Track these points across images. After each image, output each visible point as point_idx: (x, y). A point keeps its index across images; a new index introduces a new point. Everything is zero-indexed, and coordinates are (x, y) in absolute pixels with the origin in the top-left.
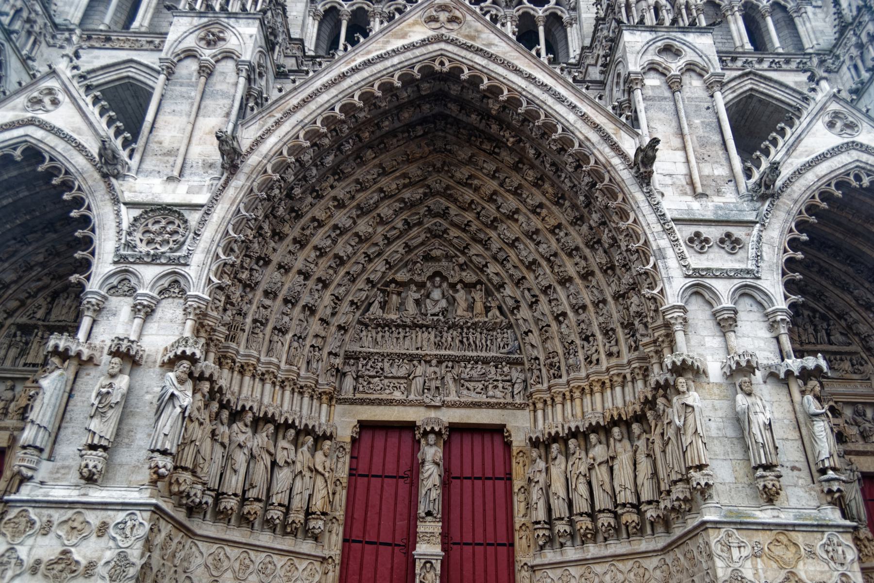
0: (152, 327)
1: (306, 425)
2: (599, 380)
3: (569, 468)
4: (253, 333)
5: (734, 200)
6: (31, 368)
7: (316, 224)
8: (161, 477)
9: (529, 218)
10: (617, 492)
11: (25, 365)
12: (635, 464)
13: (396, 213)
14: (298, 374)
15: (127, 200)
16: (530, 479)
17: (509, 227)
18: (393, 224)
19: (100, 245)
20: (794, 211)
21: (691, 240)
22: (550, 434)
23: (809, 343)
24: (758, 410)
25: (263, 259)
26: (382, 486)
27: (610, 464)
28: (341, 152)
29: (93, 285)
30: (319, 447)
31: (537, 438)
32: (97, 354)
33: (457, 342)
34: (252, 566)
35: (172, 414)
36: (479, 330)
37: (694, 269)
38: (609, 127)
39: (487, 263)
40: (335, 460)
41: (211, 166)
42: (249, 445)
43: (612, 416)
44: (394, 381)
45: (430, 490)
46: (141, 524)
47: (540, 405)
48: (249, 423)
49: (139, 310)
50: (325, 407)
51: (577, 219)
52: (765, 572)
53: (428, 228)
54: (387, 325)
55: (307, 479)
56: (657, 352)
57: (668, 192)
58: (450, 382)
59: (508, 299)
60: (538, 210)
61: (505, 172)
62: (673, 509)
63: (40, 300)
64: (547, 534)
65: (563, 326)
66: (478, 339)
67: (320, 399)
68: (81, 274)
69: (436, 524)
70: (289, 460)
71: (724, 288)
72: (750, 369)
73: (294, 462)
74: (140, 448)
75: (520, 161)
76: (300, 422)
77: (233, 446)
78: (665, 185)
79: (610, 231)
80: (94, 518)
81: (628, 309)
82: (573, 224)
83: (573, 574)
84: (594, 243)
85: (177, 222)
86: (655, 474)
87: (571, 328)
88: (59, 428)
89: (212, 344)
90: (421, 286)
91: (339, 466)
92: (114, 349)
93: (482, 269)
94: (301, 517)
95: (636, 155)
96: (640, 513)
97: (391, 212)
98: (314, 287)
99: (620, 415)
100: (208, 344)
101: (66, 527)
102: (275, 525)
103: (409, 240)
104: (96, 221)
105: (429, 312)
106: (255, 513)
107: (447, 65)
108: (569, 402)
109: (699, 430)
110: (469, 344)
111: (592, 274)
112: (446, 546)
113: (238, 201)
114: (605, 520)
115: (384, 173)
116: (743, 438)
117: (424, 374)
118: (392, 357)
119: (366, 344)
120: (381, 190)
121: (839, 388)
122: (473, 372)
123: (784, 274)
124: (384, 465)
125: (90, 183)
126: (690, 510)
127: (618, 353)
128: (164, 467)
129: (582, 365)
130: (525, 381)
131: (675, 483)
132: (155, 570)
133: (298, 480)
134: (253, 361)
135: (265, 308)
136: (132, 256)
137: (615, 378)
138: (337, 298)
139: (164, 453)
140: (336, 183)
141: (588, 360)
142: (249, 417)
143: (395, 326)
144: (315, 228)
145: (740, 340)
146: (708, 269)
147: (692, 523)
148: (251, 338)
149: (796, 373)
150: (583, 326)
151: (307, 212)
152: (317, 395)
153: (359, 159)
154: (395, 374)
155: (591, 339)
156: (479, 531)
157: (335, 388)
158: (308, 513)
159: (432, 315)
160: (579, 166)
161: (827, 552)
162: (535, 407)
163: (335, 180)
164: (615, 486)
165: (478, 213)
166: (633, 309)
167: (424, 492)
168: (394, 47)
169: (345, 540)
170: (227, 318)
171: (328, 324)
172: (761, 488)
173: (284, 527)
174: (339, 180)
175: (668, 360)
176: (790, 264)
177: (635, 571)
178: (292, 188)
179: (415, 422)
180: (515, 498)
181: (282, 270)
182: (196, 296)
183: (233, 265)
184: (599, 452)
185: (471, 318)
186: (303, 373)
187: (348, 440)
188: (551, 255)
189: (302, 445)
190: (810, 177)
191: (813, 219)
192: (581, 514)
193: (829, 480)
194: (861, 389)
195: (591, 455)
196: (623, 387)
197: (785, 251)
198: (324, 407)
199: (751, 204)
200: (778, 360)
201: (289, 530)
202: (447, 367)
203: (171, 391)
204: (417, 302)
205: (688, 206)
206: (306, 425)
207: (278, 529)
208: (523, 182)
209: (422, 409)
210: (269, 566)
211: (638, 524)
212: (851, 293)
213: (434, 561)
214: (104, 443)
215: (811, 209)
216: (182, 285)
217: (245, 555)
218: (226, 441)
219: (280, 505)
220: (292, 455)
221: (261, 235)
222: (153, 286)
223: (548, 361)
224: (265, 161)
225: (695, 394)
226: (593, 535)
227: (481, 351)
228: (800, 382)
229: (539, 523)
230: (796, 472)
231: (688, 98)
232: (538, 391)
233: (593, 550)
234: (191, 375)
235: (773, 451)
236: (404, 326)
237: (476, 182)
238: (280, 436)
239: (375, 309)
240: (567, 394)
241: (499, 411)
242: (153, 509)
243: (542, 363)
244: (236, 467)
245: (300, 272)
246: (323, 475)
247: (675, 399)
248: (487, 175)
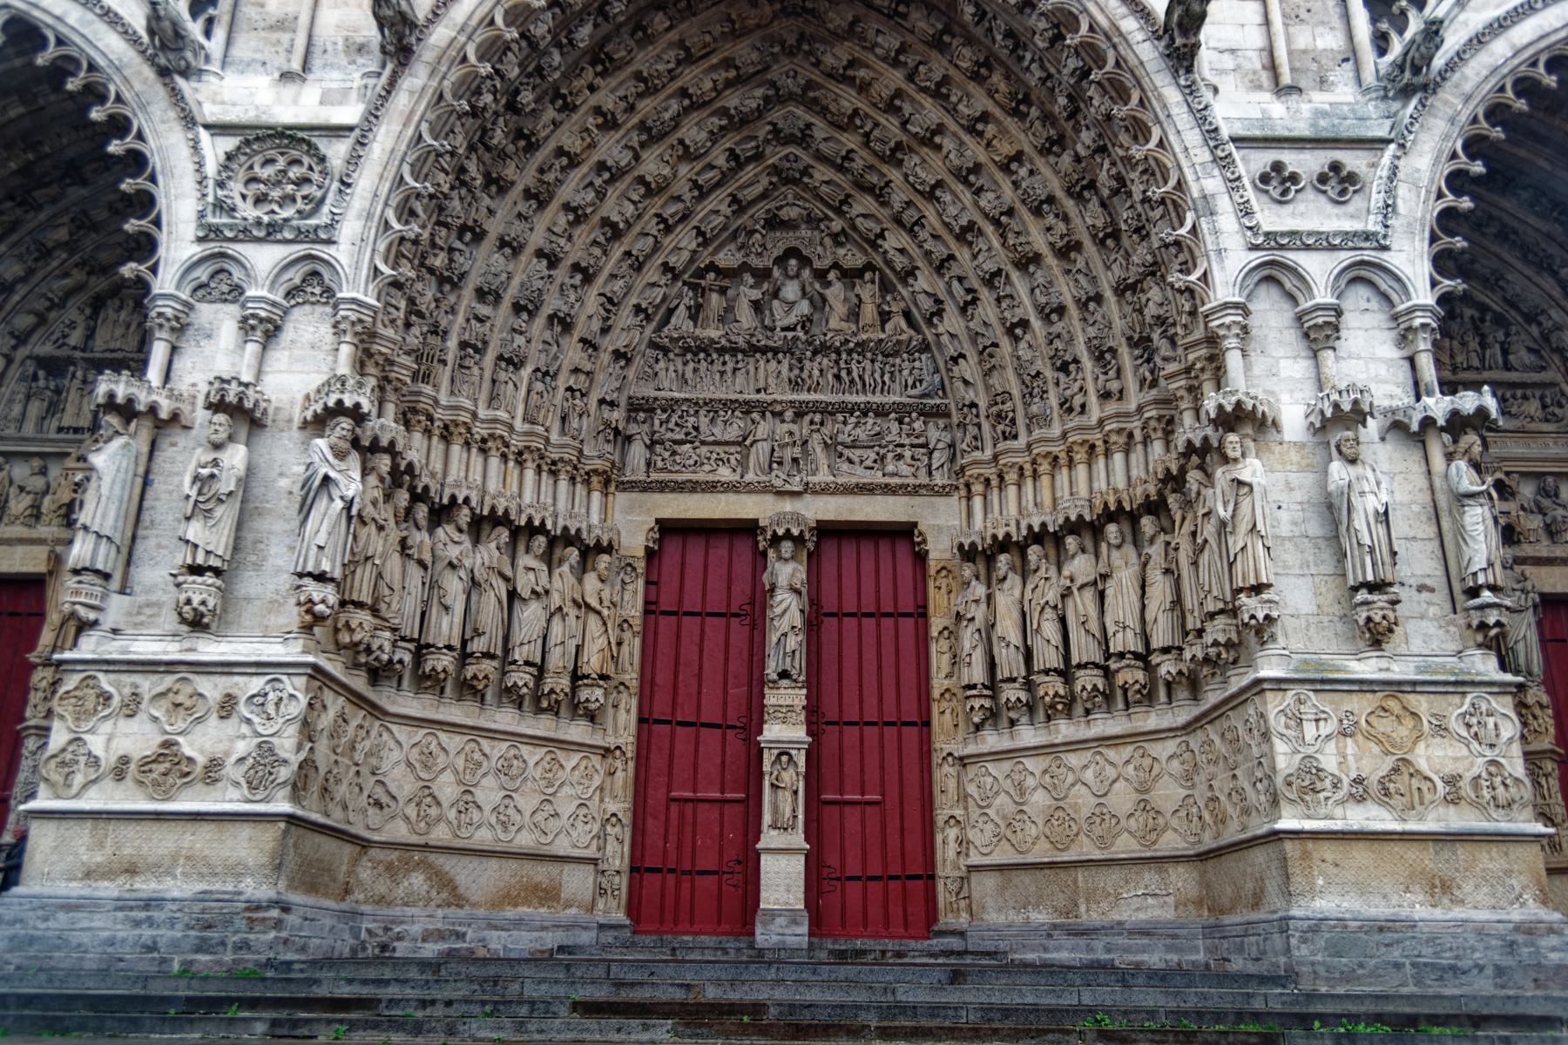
0: (279, 357)
1: (566, 529)
2: (1085, 441)
3: (1028, 595)
4: (461, 366)
5: (1351, 99)
6: (71, 436)
7: (565, 161)
8: (319, 619)
9: (962, 143)
10: (1110, 633)
11: (60, 430)
12: (1143, 587)
13: (714, 137)
14: (547, 440)
15: (210, 119)
16: (959, 616)
17: (924, 161)
18: (708, 160)
19: (169, 206)
20: (1464, 118)
21: (1265, 179)
22: (994, 537)
23: (1469, 368)
24: (1367, 489)
25: (472, 229)
26: (702, 630)
27: (1100, 587)
28: (606, 17)
29: (165, 282)
30: (589, 566)
31: (973, 544)
32: (185, 408)
33: (830, 377)
34: (485, 763)
35: (327, 513)
36: (869, 355)
37: (1267, 234)
39: (883, 230)
40: (618, 587)
41: (361, 49)
42: (467, 563)
43: (1106, 504)
44: (718, 449)
45: (785, 635)
46: (292, 696)
47: (978, 488)
48: (465, 527)
49: (253, 328)
50: (596, 496)
51: (1053, 143)
52: (1358, 759)
53: (774, 166)
54: (703, 349)
55: (571, 619)
56: (1190, 389)
57: (1227, 85)
58: (819, 449)
59: (921, 298)
60: (980, 127)
61: (917, 53)
62: (1207, 660)
63: (72, 313)
65: (1023, 345)
66: (868, 372)
67: (587, 482)
68: (140, 261)
69: (797, 691)
70: (539, 589)
71: (1319, 268)
72: (1359, 415)
73: (547, 592)
74: (278, 570)
75: (947, 30)
76: (555, 523)
77: (440, 566)
78: (1222, 72)
79: (1113, 164)
80: (212, 686)
81: (1140, 311)
82: (1044, 151)
84: (1081, 189)
85: (306, 160)
86: (1178, 602)
87: (1035, 349)
88: (134, 538)
89: (388, 388)
90: (762, 275)
91: (627, 596)
92: (214, 399)
93: (874, 242)
94: (565, 683)
95: (1169, 12)
96: (1149, 668)
97: (704, 135)
98: (568, 281)
99: (1119, 502)
100: (382, 388)
101: (165, 703)
102: (522, 697)
103: (739, 188)
104: (155, 161)
105: (779, 324)
106: (486, 677)
108: (1029, 482)
109: (1260, 526)
110: (852, 381)
111: (1078, 246)
112: (814, 727)
113: (416, 118)
114: (1087, 680)
115: (689, 59)
116: (1337, 537)
117: (771, 437)
118: (714, 408)
119: (666, 384)
120: (683, 93)
121: (1515, 448)
122: (858, 431)
123: (1433, 239)
124: (704, 595)
125: (138, 86)
126: (1235, 662)
127: (1121, 392)
128: (323, 601)
129: (1055, 415)
130: (952, 446)
131: (1212, 616)
132: (322, 771)
133: (556, 620)
134: (465, 417)
135: (480, 320)
136: (231, 227)
137: (1114, 438)
138: (610, 300)
139: (321, 578)
140: (598, 81)
141: (1066, 407)
142: (464, 517)
143: (717, 350)
144: (563, 169)
145: (1343, 364)
146: (1292, 234)
147: (1238, 681)
148: (458, 375)
149: (1441, 422)
150: (1058, 344)
151: (547, 137)
152: (582, 477)
153: (641, 33)
154: (719, 437)
155: (1072, 367)
156: (871, 701)
157: (613, 464)
158: (576, 677)
159: (783, 329)
160: (1059, 37)
161: (1469, 726)
162: (969, 491)
163: (597, 74)
165: (867, 135)
166: (1151, 310)
167: (775, 640)
169: (641, 720)
170: (414, 339)
171: (595, 348)
172: (1362, 622)
173: (537, 699)
174: (603, 74)
175: (1210, 404)
176: (1447, 220)
177: (1134, 763)
178: (517, 92)
179: (756, 521)
180: (933, 648)
181: (508, 251)
182: (354, 301)
183: (416, 242)
184: (1081, 567)
185: (854, 334)
186: (554, 437)
187: (641, 553)
188: (1002, 214)
189: (561, 562)
190: (1499, 50)
191: (1498, 133)
192: (1047, 672)
193: (1482, 607)
194: (1554, 450)
195: (1066, 572)
196: (1127, 452)
197: (1440, 195)
198: (596, 496)
199: (1382, 106)
200: (1409, 400)
201: (545, 704)
202: (812, 422)
203: (323, 470)
204: (757, 306)
205: (1264, 111)
206: (566, 529)
207: (526, 703)
208: (952, 72)
209: (769, 499)
210: (515, 762)
211: (1144, 687)
212: (1554, 274)
213: (793, 752)
214: (214, 562)
215: (1496, 113)
216: (327, 280)
217: (473, 745)
218: (427, 557)
219: (527, 663)
220: (544, 580)
221: (463, 183)
222: (273, 283)
223: (995, 409)
224: (462, 39)
225: (1257, 462)
226: (1067, 706)
227: (874, 392)
228: (1446, 437)
230: (1425, 595)
232: (975, 462)
233: (1065, 730)
234: (355, 443)
235: (1387, 559)
236: (734, 351)
237: (862, 73)
238: (521, 547)
239: (680, 320)
240: (1028, 467)
241: (906, 499)
242: (309, 671)
243: (983, 413)
244: (448, 601)
245: (540, 254)
246: (599, 613)
247: (1219, 473)
248: (884, 59)
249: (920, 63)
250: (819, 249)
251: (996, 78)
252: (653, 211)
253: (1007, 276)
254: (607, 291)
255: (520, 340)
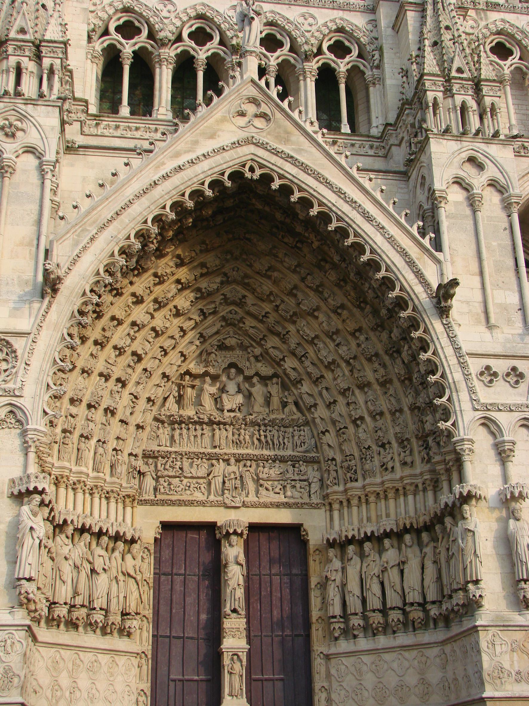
7: (115, 322)
9: (329, 317)
31: (334, 540)
38: (414, 251)
39: (284, 357)
51: (378, 326)
59: (305, 396)
60: (339, 311)
64: (342, 627)
65: (360, 430)
66: (276, 437)
70: (106, 567)
82: (373, 329)
83: (365, 661)
85: (5, 350)
86: (439, 578)
97: (188, 303)
99: (411, 524)
103: (204, 329)
106: (83, 618)
107: (258, 172)
110: (267, 442)
111: (390, 381)
122: (271, 472)
127: (412, 463)
131: (456, 591)
137: (408, 487)
138: (136, 397)
150: (380, 433)
153: (160, 254)
154: (195, 475)
155: (387, 446)
159: (228, 411)
164: (405, 588)
165: (277, 306)
168: (205, 152)
171: (127, 424)
172: (521, 598)
175: (457, 488)
181: (85, 375)
182: (35, 430)
188: (350, 358)
189: (113, 550)
192: (374, 611)
196: (415, 495)
198: (129, 510)
210: (95, 664)
211: (423, 620)
213: (240, 654)
217: (76, 655)
223: (345, 464)
229: (335, 617)
231: (488, 217)
232: (335, 492)
237: (276, 274)
244: (64, 578)
246: (135, 578)
248: (289, 269)
249: (308, 274)
250: (247, 363)
251: (348, 288)
252: (159, 345)
253: (353, 391)
254: (132, 391)
255: (91, 425)
